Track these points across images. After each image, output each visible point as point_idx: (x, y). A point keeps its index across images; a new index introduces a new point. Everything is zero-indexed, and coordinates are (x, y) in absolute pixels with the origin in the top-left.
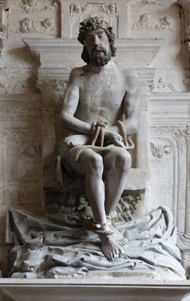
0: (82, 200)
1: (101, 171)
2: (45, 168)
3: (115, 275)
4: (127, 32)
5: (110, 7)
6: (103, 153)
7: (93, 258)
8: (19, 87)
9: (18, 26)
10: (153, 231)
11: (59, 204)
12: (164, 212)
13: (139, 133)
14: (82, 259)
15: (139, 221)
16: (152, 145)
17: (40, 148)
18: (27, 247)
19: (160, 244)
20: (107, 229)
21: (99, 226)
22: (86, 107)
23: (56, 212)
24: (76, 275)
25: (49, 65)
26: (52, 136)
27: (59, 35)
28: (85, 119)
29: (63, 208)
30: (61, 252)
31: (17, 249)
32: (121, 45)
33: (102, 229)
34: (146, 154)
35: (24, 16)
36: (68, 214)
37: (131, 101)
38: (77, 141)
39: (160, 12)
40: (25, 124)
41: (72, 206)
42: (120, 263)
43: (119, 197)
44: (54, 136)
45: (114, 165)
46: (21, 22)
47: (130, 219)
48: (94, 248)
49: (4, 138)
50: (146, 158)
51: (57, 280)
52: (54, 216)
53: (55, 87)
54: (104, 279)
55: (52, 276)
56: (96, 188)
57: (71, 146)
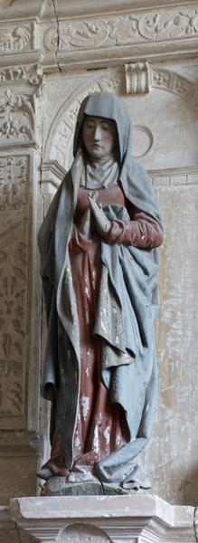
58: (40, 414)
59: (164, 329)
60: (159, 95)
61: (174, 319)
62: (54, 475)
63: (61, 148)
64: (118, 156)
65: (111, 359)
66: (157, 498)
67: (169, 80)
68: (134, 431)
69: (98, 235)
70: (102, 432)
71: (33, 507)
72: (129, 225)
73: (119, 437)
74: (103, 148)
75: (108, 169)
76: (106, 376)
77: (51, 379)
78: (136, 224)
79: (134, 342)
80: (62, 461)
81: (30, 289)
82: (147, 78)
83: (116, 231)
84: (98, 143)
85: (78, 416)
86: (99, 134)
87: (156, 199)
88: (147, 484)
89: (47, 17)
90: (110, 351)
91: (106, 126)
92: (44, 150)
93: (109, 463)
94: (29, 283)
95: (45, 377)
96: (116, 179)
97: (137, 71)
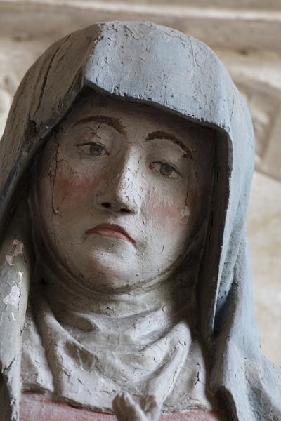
64: (198, 295)
74: (140, 246)
84: (126, 222)
86: (135, 184)
91: (173, 156)
96: (199, 387)
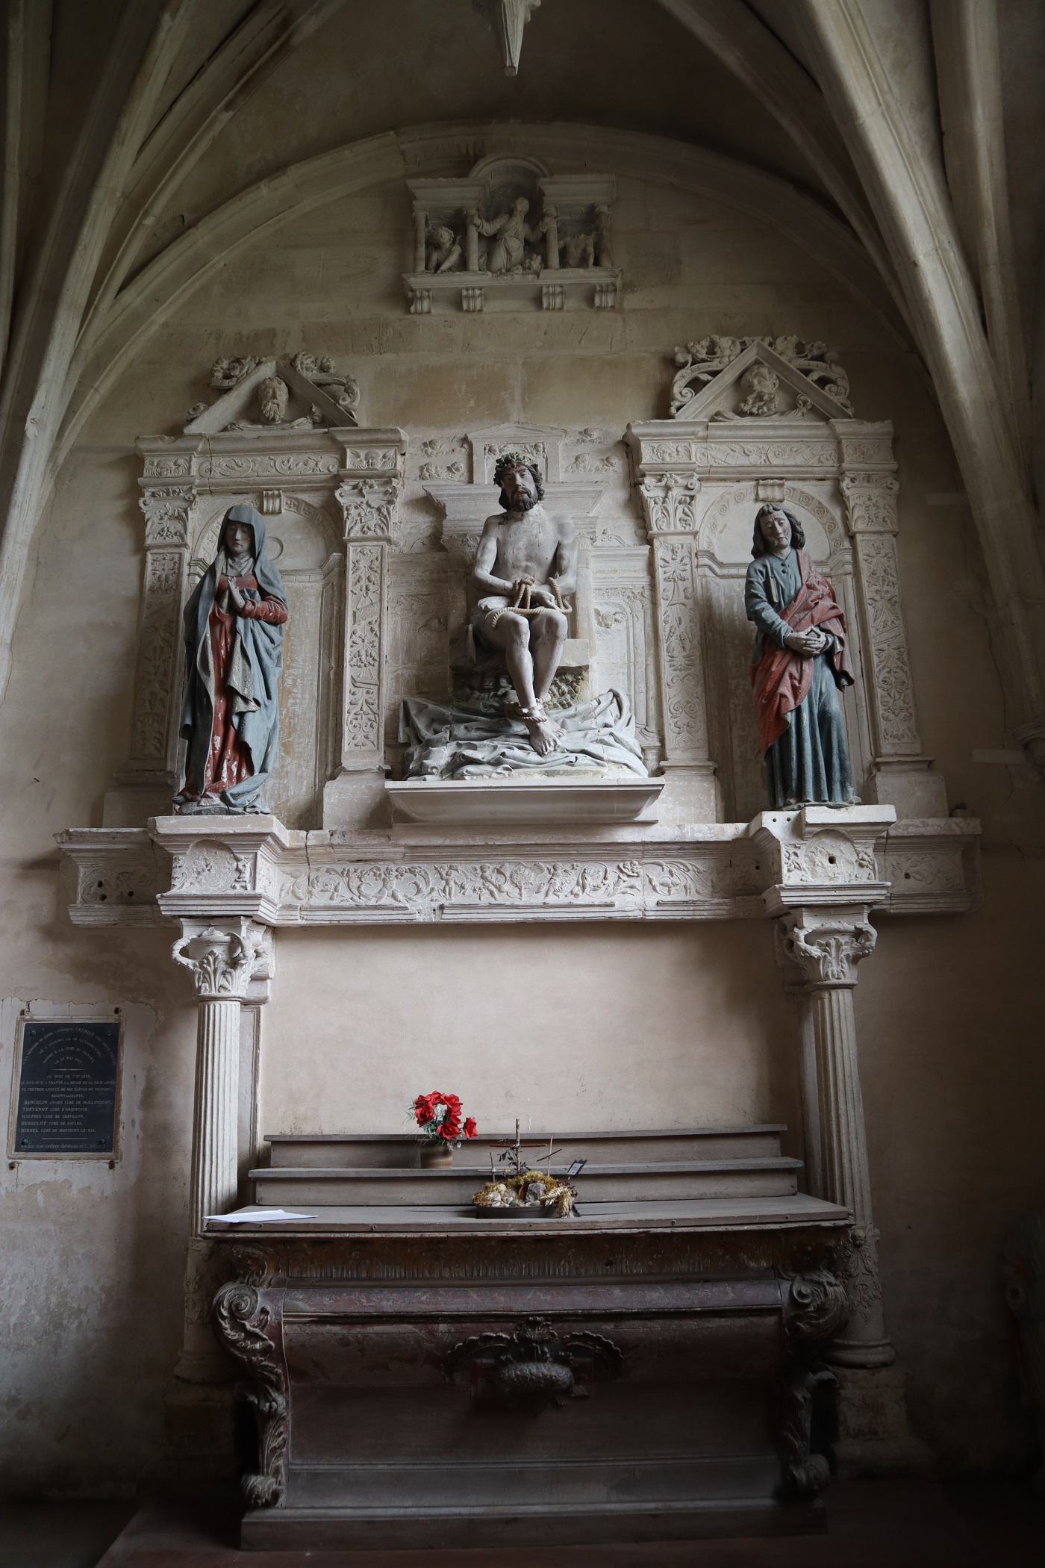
0: (504, 682)
1: (526, 638)
2: (453, 641)
3: (548, 774)
4: (559, 473)
5: (536, 446)
6: (531, 618)
7: (518, 753)
8: (419, 544)
9: (418, 473)
10: (601, 720)
11: (472, 689)
12: (616, 696)
13: (578, 596)
14: (503, 754)
15: (581, 707)
16: (598, 613)
17: (446, 619)
18: (427, 745)
19: (611, 734)
20: (537, 714)
21: (525, 711)
22: (505, 563)
23: (468, 698)
24: (494, 775)
25: (458, 517)
26: (461, 601)
27: (471, 481)
28: (507, 578)
29: (477, 694)
30: (475, 748)
31: (416, 751)
32: (552, 490)
33: (530, 714)
34: (588, 622)
35: (425, 460)
36: (485, 701)
37: (566, 553)
38: (495, 604)
39: (601, 452)
40: (425, 591)
41: (489, 690)
42: (554, 758)
43: (551, 676)
44: (464, 603)
45: (544, 630)
46: (421, 468)
47: (569, 705)
48: (520, 742)
49: (398, 608)
50: (590, 629)
51: (469, 782)
52: (465, 705)
53: (465, 542)
54: (533, 779)
55: (462, 777)
56: (520, 659)
57: (487, 610)
58: (179, 746)
59: (286, 693)
60: (288, 515)
61: (294, 685)
62: (188, 800)
63: (208, 549)
64: (253, 553)
65: (240, 706)
66: (274, 818)
67: (298, 504)
68: (257, 767)
69: (235, 611)
70: (230, 766)
71: (167, 825)
72: (259, 604)
73: (244, 771)
75: (245, 564)
76: (235, 720)
77: (188, 721)
78: (266, 604)
79: (261, 695)
80: (194, 789)
81: (175, 656)
82: (283, 503)
83: (249, 607)
85: (210, 752)
86: (239, 535)
87: (282, 588)
88: (267, 810)
89: (203, 453)
90: (239, 700)
92: (194, 550)
93: (236, 790)
94: (175, 652)
95: (183, 719)
97: (273, 497)
